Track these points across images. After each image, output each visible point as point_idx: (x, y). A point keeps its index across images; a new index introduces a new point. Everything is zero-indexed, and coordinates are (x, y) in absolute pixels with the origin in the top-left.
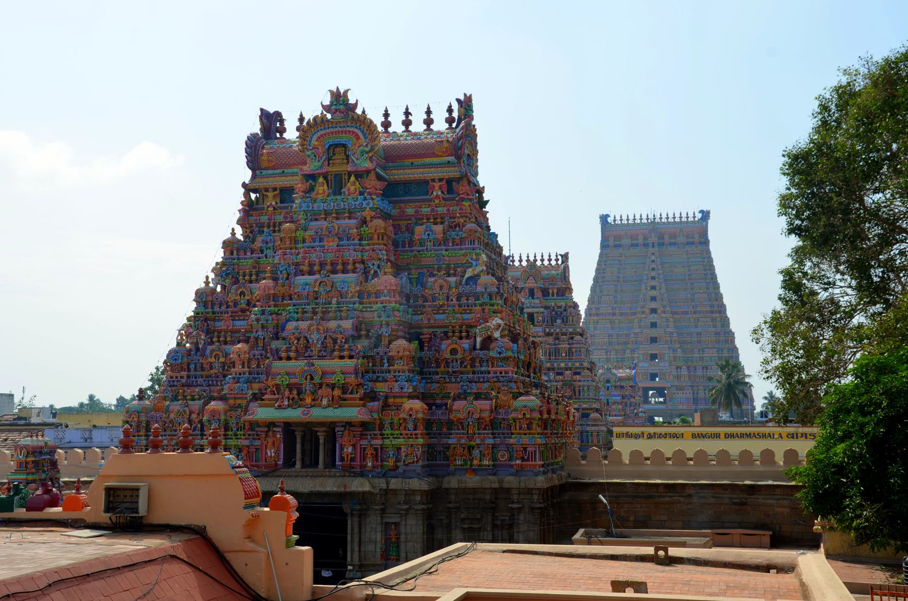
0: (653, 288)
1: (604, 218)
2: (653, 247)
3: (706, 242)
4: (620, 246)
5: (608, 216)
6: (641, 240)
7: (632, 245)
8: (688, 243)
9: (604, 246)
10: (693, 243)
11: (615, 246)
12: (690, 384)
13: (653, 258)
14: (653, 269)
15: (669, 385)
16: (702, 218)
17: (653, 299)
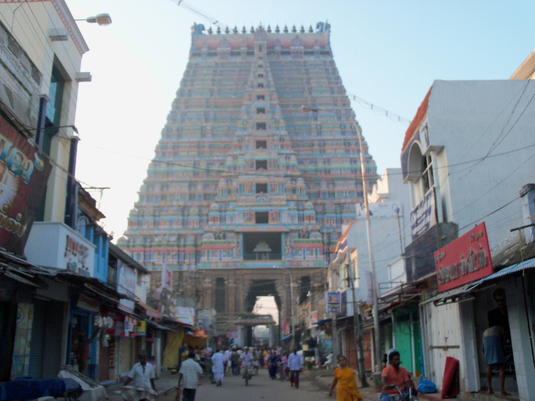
0: (261, 97)
1: (198, 29)
2: (260, 50)
3: (329, 53)
4: (215, 54)
5: (202, 27)
6: (244, 49)
7: (233, 54)
8: (306, 53)
9: (195, 53)
10: (312, 53)
11: (210, 54)
12: (318, 227)
13: (261, 62)
14: (261, 76)
15: (285, 229)
16: (321, 31)
17: (261, 111)
